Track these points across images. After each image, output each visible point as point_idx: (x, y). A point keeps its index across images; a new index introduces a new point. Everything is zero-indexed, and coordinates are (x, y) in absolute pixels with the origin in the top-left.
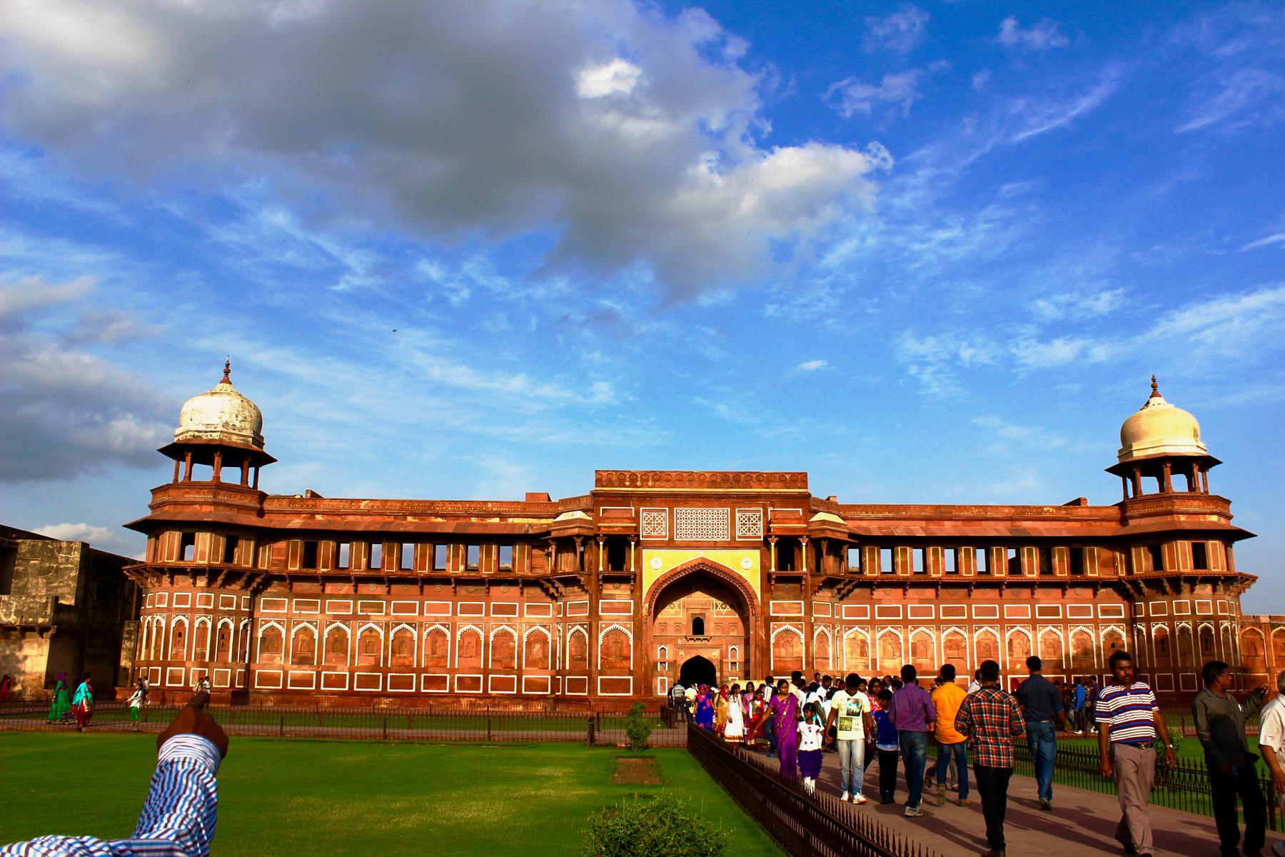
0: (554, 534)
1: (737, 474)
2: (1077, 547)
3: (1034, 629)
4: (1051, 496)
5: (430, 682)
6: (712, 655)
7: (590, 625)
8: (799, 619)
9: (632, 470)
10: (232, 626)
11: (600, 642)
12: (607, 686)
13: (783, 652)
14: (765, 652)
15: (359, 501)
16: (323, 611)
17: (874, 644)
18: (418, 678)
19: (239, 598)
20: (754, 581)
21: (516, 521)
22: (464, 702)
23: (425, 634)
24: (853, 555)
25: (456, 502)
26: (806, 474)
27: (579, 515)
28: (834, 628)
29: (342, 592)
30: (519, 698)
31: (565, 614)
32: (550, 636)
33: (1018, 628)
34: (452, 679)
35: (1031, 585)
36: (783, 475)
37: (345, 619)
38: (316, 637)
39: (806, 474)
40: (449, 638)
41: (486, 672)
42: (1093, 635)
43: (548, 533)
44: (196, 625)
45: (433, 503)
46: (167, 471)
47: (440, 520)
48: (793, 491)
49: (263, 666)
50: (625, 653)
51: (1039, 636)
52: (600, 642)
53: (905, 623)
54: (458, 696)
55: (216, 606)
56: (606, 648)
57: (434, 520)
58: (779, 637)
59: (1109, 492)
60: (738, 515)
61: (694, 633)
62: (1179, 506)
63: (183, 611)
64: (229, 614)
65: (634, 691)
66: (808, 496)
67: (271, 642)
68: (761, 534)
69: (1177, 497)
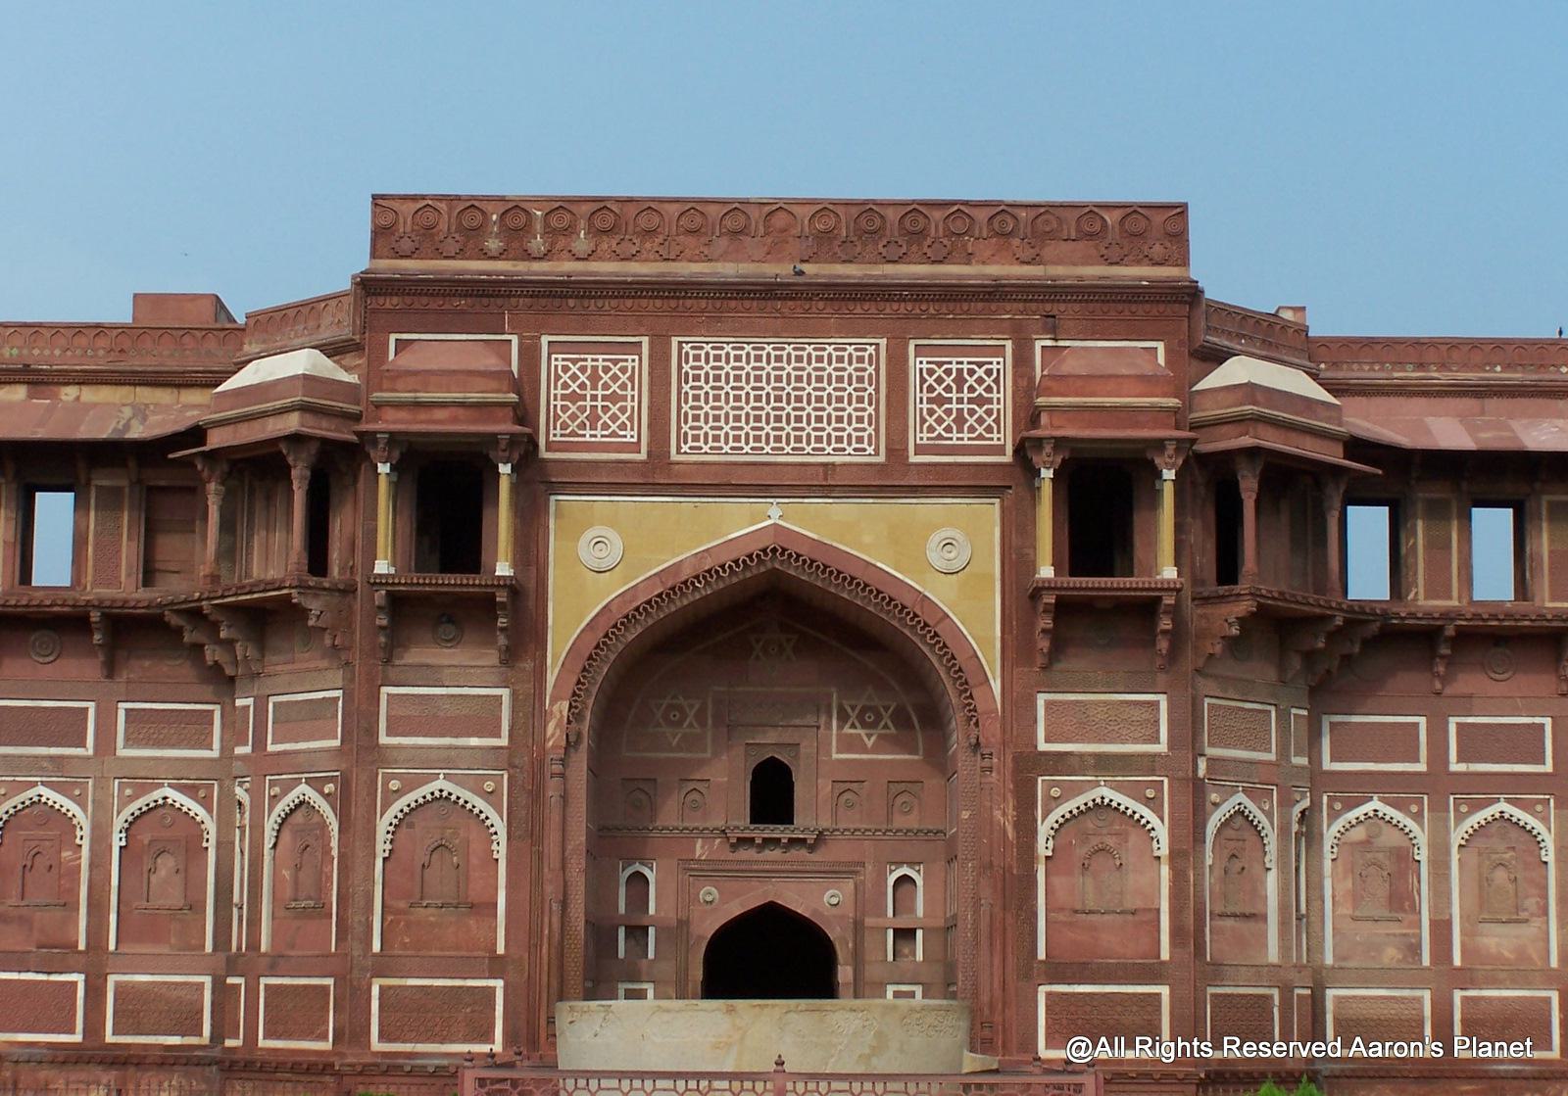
0: (216, 440)
6: (822, 901)
7: (345, 784)
11: (382, 847)
13: (1085, 890)
14: (1017, 890)
17: (1440, 865)
21: (89, 394)
24: (1367, 528)
26: (1180, 211)
27: (301, 362)
28: (1286, 802)
31: (260, 743)
32: (211, 826)
39: (1180, 211)
43: (196, 434)
48: (1127, 267)
50: (475, 893)
52: (382, 847)
60: (917, 364)
61: (758, 816)
66: (1191, 294)
68: (1005, 437)
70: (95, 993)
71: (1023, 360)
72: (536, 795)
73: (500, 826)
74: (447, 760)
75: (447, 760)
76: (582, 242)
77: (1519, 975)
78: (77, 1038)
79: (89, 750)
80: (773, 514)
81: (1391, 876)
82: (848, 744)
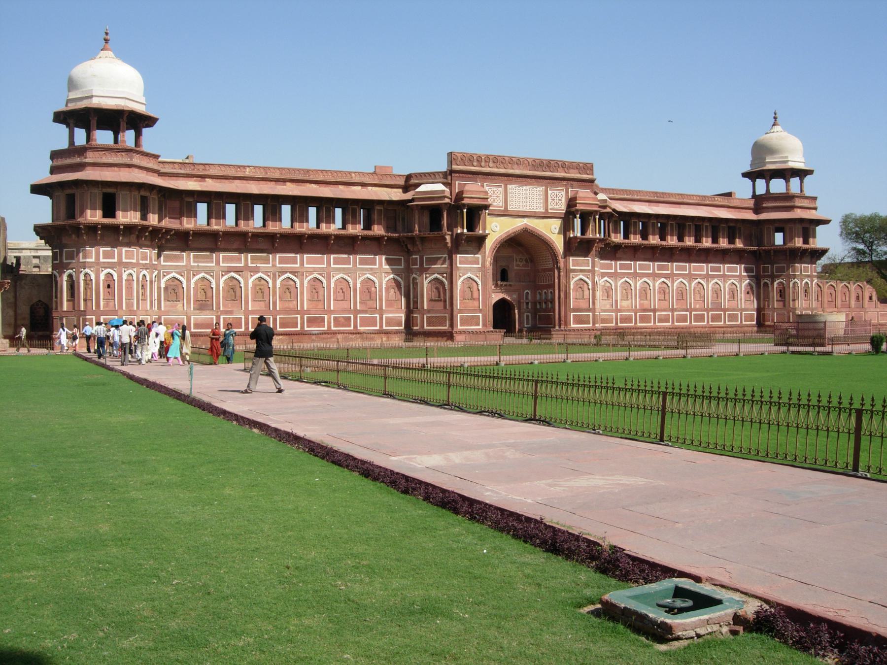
1: (549, 161)
2: (732, 228)
3: (708, 281)
4: (710, 189)
5: (311, 321)
8: (588, 271)
9: (479, 152)
10: (148, 279)
12: (465, 321)
15: (244, 167)
16: (218, 263)
17: (616, 289)
18: (302, 319)
19: (151, 253)
20: (558, 243)
21: (374, 189)
22: (339, 336)
25: (327, 171)
26: (592, 165)
27: (440, 187)
29: (235, 246)
30: (381, 332)
34: (329, 319)
35: (707, 251)
36: (578, 164)
37: (238, 271)
38: (214, 285)
40: (325, 285)
41: (356, 312)
44: (125, 277)
45: (308, 171)
47: (313, 185)
49: (167, 312)
51: (710, 285)
52: (459, 287)
53: (635, 275)
54: (335, 333)
55: (138, 260)
56: (463, 292)
57: (308, 185)
58: (576, 283)
59: (744, 190)
60: (550, 192)
62: (798, 202)
63: (112, 266)
64: (145, 267)
65: (484, 325)
66: (592, 181)
67: (174, 291)
68: (564, 207)
69: (798, 197)
70: (381, 319)
71: (567, 192)
73: (479, 282)
74: (470, 270)
75: (470, 270)
76: (491, 164)
77: (628, 310)
78: (378, 328)
80: (525, 221)
81: (608, 292)
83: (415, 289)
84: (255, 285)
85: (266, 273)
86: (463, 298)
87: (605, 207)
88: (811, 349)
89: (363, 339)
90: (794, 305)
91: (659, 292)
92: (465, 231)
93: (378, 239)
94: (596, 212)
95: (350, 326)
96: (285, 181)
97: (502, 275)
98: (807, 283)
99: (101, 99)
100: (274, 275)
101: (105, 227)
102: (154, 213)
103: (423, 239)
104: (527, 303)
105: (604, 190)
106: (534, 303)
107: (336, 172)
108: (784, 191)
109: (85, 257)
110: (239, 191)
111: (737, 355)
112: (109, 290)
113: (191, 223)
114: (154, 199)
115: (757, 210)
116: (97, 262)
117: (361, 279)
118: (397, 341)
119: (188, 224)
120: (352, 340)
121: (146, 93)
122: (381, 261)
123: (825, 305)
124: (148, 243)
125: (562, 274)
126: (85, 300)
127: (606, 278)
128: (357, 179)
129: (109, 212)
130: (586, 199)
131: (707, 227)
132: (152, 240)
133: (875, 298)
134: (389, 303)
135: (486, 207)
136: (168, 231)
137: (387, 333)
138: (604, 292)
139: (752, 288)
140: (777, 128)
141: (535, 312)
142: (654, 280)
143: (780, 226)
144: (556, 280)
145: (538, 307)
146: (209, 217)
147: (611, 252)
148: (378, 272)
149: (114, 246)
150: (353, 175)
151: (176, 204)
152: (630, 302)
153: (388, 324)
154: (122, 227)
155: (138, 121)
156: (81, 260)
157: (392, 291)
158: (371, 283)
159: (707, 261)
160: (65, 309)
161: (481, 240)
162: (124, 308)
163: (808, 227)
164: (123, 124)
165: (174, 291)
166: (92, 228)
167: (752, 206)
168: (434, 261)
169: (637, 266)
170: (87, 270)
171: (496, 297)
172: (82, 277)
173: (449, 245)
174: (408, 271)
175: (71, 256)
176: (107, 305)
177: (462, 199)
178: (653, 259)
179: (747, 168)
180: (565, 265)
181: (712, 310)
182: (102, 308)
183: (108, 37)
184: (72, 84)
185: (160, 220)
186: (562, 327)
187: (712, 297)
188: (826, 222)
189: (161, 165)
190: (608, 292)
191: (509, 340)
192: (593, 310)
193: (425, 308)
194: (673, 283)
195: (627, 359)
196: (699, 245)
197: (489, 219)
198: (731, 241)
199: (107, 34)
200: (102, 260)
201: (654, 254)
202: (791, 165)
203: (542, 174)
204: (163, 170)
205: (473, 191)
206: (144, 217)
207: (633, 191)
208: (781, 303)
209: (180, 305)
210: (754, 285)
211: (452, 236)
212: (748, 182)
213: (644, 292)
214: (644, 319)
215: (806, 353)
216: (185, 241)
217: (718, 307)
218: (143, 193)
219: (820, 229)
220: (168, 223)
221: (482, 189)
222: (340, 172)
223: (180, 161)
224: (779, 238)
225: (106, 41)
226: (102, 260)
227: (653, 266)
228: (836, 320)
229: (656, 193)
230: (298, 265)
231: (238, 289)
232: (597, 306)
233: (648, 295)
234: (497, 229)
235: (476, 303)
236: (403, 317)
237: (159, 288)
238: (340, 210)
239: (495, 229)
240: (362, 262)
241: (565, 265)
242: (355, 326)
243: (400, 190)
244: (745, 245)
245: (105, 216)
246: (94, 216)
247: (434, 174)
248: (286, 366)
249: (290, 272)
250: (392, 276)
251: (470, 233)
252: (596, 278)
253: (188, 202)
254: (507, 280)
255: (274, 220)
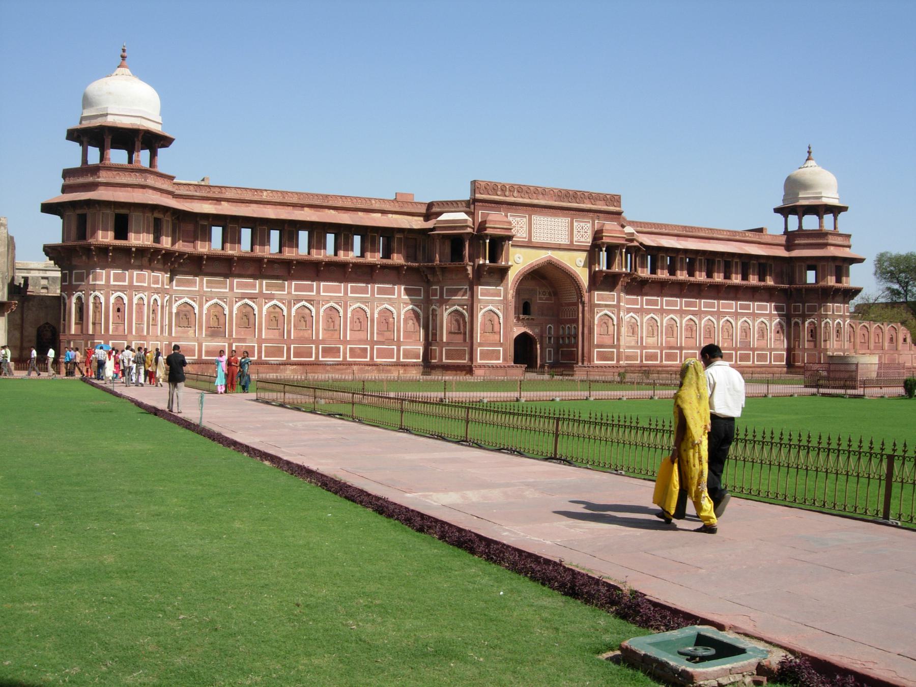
1: (576, 192)
2: (763, 265)
3: (736, 319)
5: (327, 351)
8: (613, 306)
10: (159, 303)
12: (484, 355)
15: (261, 191)
16: (231, 289)
18: (317, 349)
19: (163, 277)
20: (584, 277)
21: (395, 216)
22: (355, 368)
23: (322, 311)
25: (346, 197)
26: (620, 197)
27: (462, 216)
29: (249, 272)
30: (398, 364)
33: (727, 318)
34: (345, 349)
36: (605, 195)
37: (252, 298)
38: (227, 312)
40: (341, 314)
41: (373, 343)
42: (768, 324)
44: (135, 301)
45: (327, 196)
46: (72, 155)
51: (739, 323)
53: (662, 311)
54: (350, 364)
56: (484, 324)
57: (327, 210)
59: (775, 226)
60: (575, 224)
62: (831, 240)
63: (122, 289)
64: (157, 291)
65: (505, 359)
66: (619, 213)
67: (185, 316)
68: (590, 240)
69: (831, 234)
70: (399, 350)
71: (593, 224)
72: (507, 309)
73: (501, 315)
74: (492, 302)
75: (492, 302)
77: (654, 348)
78: (395, 360)
79: (396, 296)
81: (633, 328)
82: (540, 299)
83: (434, 321)
84: (269, 313)
85: (280, 300)
86: (484, 331)
87: (632, 240)
88: (842, 391)
89: (379, 371)
90: (825, 346)
91: (686, 330)
92: (487, 262)
93: (397, 268)
94: (623, 245)
95: (366, 357)
96: (302, 206)
97: (524, 308)
98: (839, 323)
99: (116, 118)
100: (290, 303)
101: (117, 249)
102: (167, 236)
103: (444, 270)
104: (550, 338)
105: (632, 223)
106: (557, 338)
107: (356, 198)
108: (817, 227)
109: (95, 279)
110: (255, 215)
111: (765, 396)
112: (119, 314)
113: (204, 247)
114: (168, 221)
115: (789, 246)
116: (108, 285)
117: (379, 309)
118: (415, 374)
119: (202, 248)
120: (368, 371)
121: (162, 113)
122: (400, 292)
123: (858, 347)
124: (160, 266)
125: (586, 308)
126: (94, 324)
127: (632, 314)
128: (377, 206)
129: (121, 233)
130: (613, 232)
131: (736, 263)
132: (165, 263)
133: (909, 340)
134: (408, 334)
135: (510, 238)
136: (181, 254)
137: (404, 365)
138: (629, 328)
139: (782, 327)
140: (811, 163)
141: (557, 347)
142: (681, 317)
143: (812, 263)
144: (580, 315)
145: (561, 342)
146: (224, 241)
147: (638, 287)
148: (397, 302)
149: (126, 268)
150: (373, 202)
151: (190, 227)
152: (655, 339)
153: (405, 356)
154: (134, 249)
155: (154, 141)
156: (91, 282)
157: (411, 322)
158: (388, 314)
159: (736, 299)
160: (73, 332)
161: (503, 272)
162: (134, 333)
163: (841, 265)
164: (138, 144)
165: (185, 316)
166: (104, 250)
167: (784, 242)
168: (455, 292)
169: (664, 302)
170: (97, 293)
171: (518, 331)
172: (91, 300)
173: (471, 276)
174: (428, 302)
175: (81, 278)
176: (116, 329)
177: (485, 229)
178: (681, 295)
179: (779, 204)
180: (590, 300)
181: (740, 349)
182: (111, 332)
183: (125, 54)
184: (87, 101)
185: (173, 243)
186: (586, 364)
187: (741, 335)
188: (860, 261)
189: (176, 187)
190: (633, 328)
191: (531, 376)
192: (618, 347)
193: (445, 340)
194: (700, 320)
195: (651, 398)
196: (728, 282)
197: (512, 250)
198: (762, 279)
199: (124, 51)
200: (112, 283)
201: (681, 290)
202: (825, 201)
203: (568, 205)
204: (177, 192)
205: (496, 220)
206: (157, 240)
207: (661, 225)
208: (812, 343)
209: (191, 331)
210: (784, 325)
211: (473, 266)
212: (780, 218)
213: (671, 330)
214: (670, 357)
215: (837, 396)
216: (198, 265)
217: (746, 346)
218: (157, 215)
219: (853, 268)
220: (181, 246)
221: (505, 219)
222: (360, 198)
223: (196, 183)
224: (811, 277)
225: (123, 58)
226: (112, 283)
227: (680, 303)
228: (869, 362)
229: (685, 227)
230: (314, 293)
231: (252, 316)
232: (622, 343)
233: (675, 333)
234: (521, 261)
235: (497, 337)
236: (421, 349)
237: (170, 313)
238: (359, 237)
239: (519, 261)
240: (380, 291)
241: (590, 300)
242: (372, 358)
243: (422, 219)
244: (775, 283)
245: (116, 238)
246: (105, 237)
247: (456, 202)
248: (299, 397)
249: (306, 301)
250: (411, 307)
251: (492, 264)
252: (622, 314)
253: (203, 226)
254: (529, 314)
255: (291, 246)
